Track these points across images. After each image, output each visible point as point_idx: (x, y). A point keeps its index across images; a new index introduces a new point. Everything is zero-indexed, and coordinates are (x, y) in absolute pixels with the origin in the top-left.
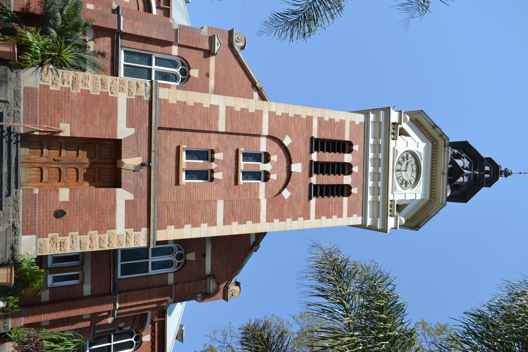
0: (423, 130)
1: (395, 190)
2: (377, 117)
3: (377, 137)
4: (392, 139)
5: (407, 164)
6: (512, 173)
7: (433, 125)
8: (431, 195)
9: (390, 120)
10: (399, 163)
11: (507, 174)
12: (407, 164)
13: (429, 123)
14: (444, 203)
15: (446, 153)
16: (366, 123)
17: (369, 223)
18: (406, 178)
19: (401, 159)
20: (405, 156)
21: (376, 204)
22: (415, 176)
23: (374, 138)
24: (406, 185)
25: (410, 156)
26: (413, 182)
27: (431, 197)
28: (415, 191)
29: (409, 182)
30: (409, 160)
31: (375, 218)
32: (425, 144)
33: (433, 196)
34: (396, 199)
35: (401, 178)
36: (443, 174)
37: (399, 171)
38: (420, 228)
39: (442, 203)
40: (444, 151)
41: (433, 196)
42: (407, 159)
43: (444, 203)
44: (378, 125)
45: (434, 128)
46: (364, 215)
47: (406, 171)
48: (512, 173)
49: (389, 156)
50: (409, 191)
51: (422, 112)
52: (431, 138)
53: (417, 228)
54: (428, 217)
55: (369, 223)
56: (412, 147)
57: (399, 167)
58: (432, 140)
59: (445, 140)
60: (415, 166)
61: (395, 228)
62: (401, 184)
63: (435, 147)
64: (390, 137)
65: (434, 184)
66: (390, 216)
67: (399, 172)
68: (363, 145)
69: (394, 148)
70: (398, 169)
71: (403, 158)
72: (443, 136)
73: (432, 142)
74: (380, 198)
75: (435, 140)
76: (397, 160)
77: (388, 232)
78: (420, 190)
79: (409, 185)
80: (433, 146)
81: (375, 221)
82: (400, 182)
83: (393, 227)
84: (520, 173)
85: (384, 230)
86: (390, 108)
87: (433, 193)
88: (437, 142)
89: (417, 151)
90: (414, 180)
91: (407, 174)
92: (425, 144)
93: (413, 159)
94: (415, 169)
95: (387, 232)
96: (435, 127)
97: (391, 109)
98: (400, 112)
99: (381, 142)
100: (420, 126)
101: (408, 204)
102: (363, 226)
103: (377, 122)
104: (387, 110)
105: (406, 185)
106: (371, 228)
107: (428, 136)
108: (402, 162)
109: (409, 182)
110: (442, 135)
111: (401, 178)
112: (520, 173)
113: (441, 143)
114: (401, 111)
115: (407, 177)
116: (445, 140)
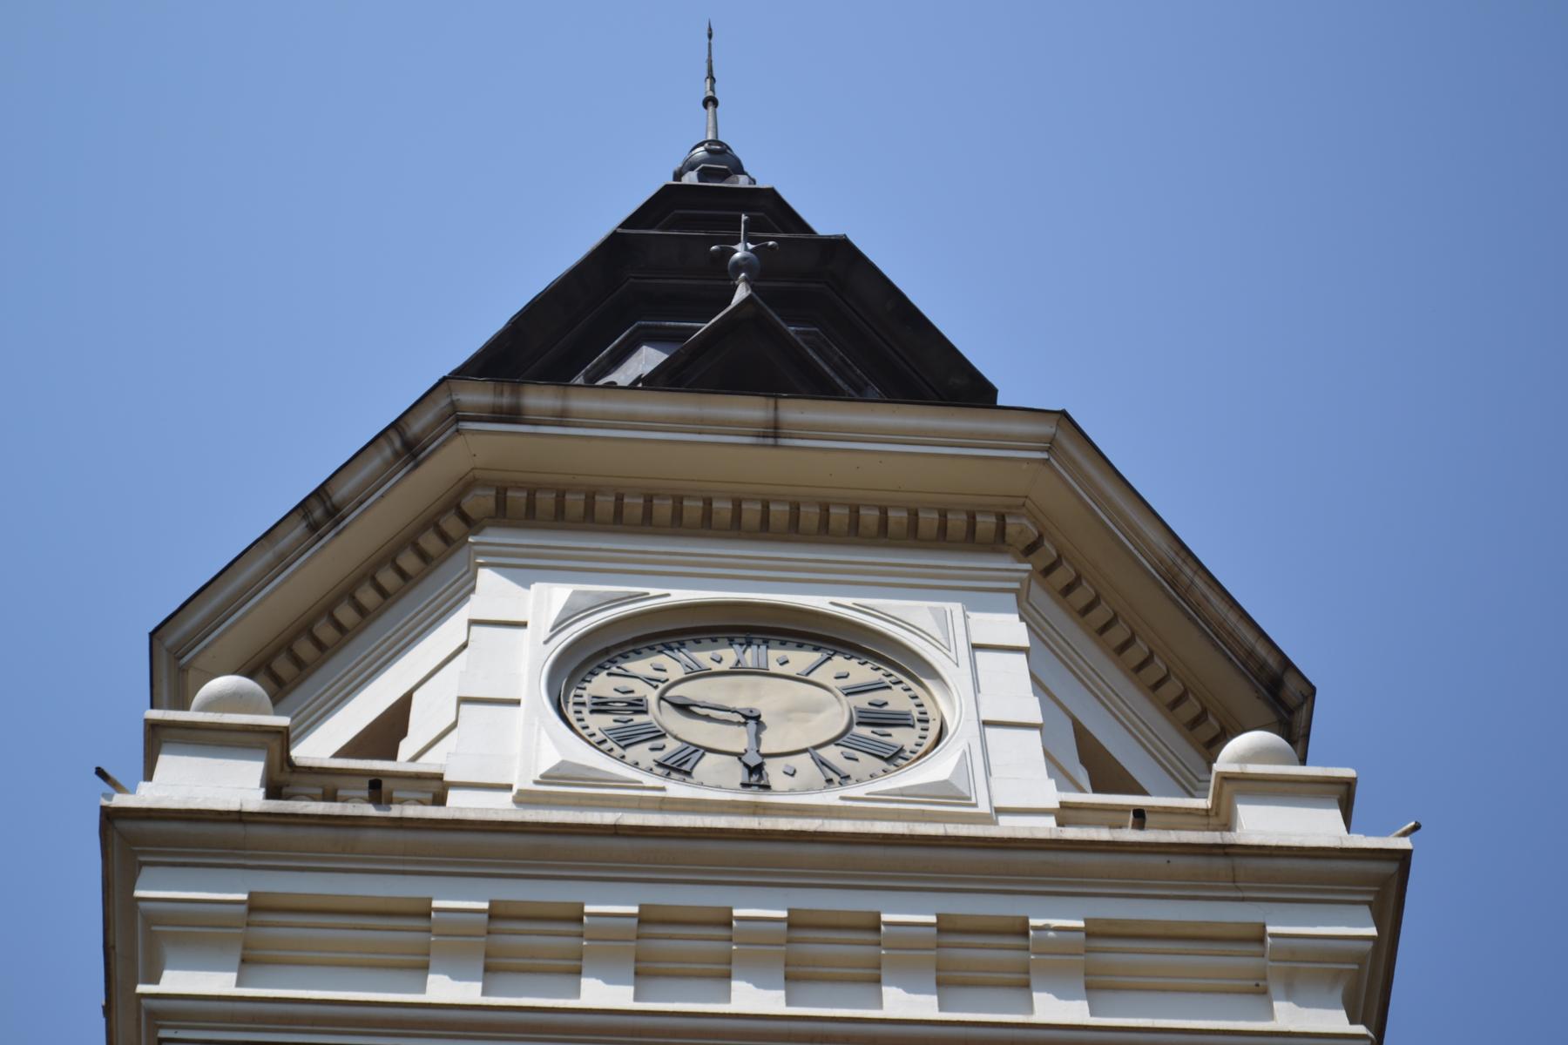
0: (346, 614)
1: (963, 799)
2: (198, 933)
4: (440, 800)
5: (684, 708)
6: (716, 142)
7: (299, 529)
8: (970, 541)
9: (240, 817)
12: (684, 708)
13: (282, 562)
14: (1046, 429)
18: (834, 716)
21: (1119, 957)
22: (801, 659)
23: (424, 968)
24: (901, 720)
25: (602, 685)
26: (862, 672)
27: (998, 542)
28: (945, 648)
29: (862, 701)
32: (486, 577)
33: (986, 523)
34: (1050, 795)
35: (832, 754)
36: (774, 431)
37: (757, 770)
38: (1287, 664)
39: (1051, 445)
41: (986, 523)
42: (638, 706)
43: (1046, 429)
44: (277, 932)
45: (335, 514)
47: (753, 719)
48: (716, 142)
49: (616, 831)
50: (953, 705)
51: (173, 638)
52: (431, 542)
53: (1291, 684)
54: (1183, 578)
56: (525, 663)
58: (451, 524)
59: (456, 415)
60: (704, 657)
61: (1344, 795)
62: (894, 758)
63: (517, 497)
64: (412, 811)
65: (870, 516)
66: (1228, 826)
67: (773, 769)
70: (740, 774)
71: (627, 739)
72: (416, 427)
73: (472, 524)
74: (1056, 918)
75: (454, 505)
76: (649, 780)
77: (1405, 843)
78: (943, 620)
79: (897, 700)
80: (502, 515)
81: (1305, 969)
82: (868, 763)
83: (1336, 814)
84: (710, 102)
85: (1383, 882)
86: (110, 817)
87: (957, 521)
88: (468, 484)
89: (559, 626)
90: (839, 663)
91: (788, 713)
92: (486, 577)
93: (641, 666)
94: (729, 656)
95: (1404, 857)
96: (321, 511)
97: (120, 801)
98: (158, 738)
99: (460, 900)
100: (305, 649)
103: (249, 936)
104: (132, 839)
105: (901, 720)
107: (409, 562)
108: (671, 745)
109: (862, 701)
110: (403, 443)
111: (832, 754)
112: (710, 102)
113: (480, 448)
114: (153, 728)
115: (817, 709)
116: (456, 415)
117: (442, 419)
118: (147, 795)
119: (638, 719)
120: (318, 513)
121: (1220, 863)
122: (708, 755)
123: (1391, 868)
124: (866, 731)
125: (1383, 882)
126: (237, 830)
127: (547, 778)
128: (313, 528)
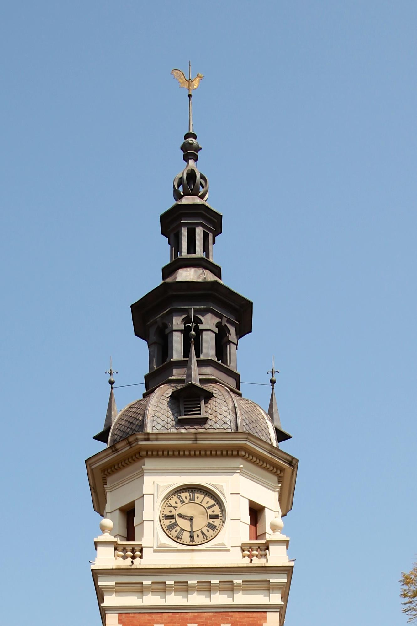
3: (141, 590)
7: (110, 451)
10: (178, 539)
11: (191, 183)
12: (180, 516)
13: (108, 455)
15: (160, 437)
16: (122, 611)
17: (276, 599)
19: (174, 533)
20: (167, 522)
22: (200, 496)
26: (212, 502)
27: (238, 456)
30: (175, 513)
31: (268, 588)
38: (293, 458)
40: (157, 440)
42: (172, 517)
46: (263, 609)
51: (89, 462)
53: (294, 462)
55: (276, 599)
57: (186, 537)
68: (154, 616)
69: (155, 551)
73: (142, 457)
77: (292, 564)
80: (147, 456)
85: (288, 571)
86: (92, 570)
90: (207, 499)
95: (293, 567)
97: (93, 567)
101: (251, 503)
102: (282, 610)
104: (96, 574)
106: (285, 597)
117: (135, 440)
118: (98, 564)
119: (173, 521)
120: (114, 449)
121: (264, 569)
122: (185, 532)
123: (290, 568)
124: (211, 521)
125: (289, 570)
126: (112, 571)
127: (159, 546)
128: (113, 451)
